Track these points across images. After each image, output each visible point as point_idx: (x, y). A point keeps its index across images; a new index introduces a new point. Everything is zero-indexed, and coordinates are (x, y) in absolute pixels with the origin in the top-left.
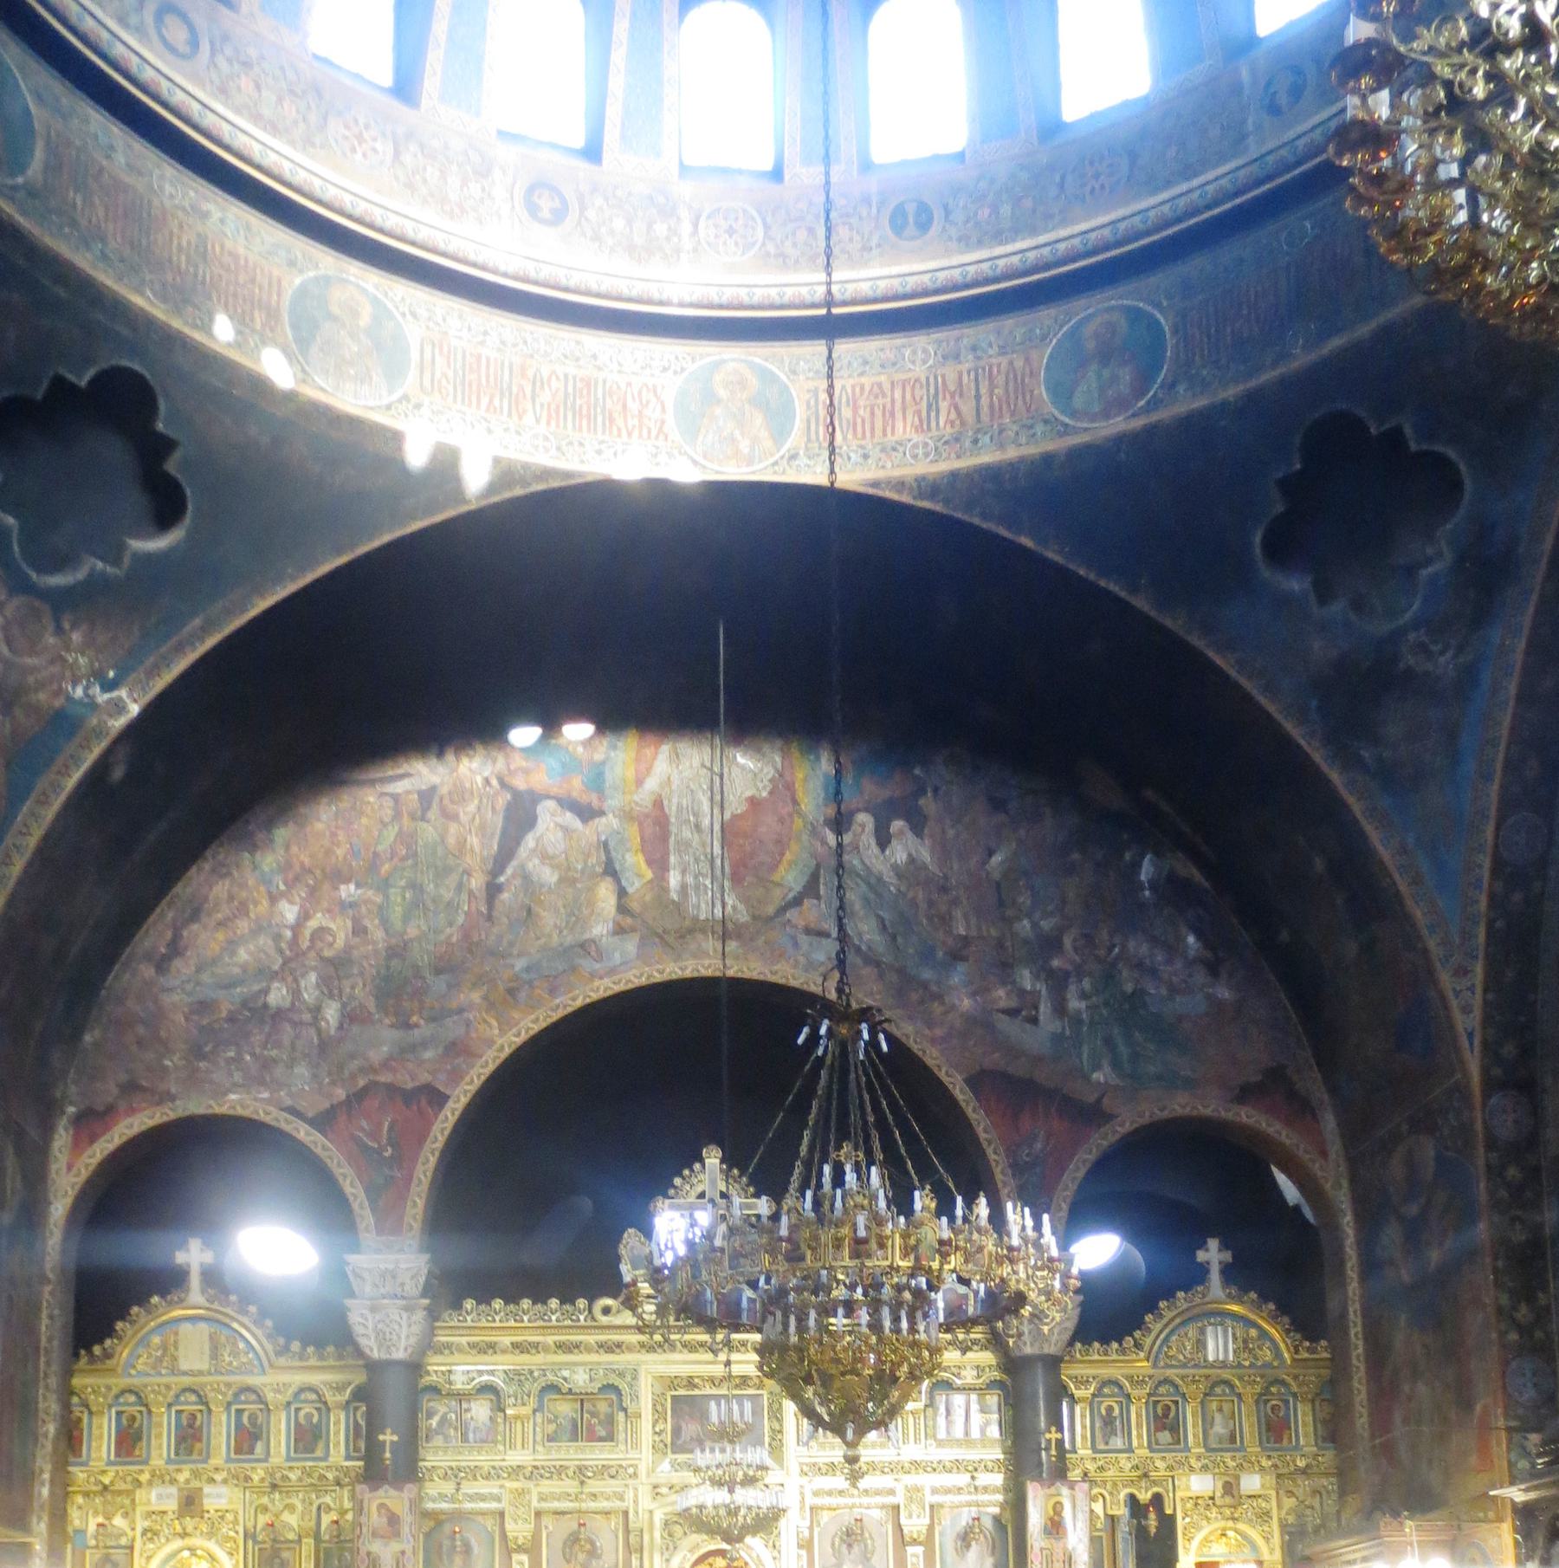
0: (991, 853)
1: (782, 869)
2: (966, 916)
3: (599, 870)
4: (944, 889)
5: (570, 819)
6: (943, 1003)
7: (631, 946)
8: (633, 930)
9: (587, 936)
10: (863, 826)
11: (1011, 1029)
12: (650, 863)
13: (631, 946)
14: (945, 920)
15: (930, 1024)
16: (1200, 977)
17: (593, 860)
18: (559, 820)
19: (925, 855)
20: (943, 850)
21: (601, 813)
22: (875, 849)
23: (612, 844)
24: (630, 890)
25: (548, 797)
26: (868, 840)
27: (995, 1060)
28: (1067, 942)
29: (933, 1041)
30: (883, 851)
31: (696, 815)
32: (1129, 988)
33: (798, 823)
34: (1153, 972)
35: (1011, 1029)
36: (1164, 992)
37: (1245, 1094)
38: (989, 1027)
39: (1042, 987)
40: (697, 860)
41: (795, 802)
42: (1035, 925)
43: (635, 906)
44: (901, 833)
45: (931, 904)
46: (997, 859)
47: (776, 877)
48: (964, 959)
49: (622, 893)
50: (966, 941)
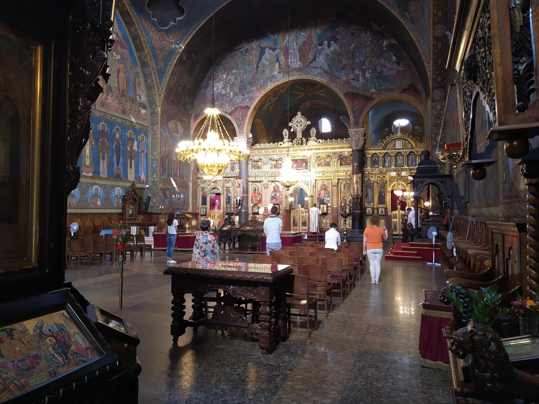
0: (351, 45)
1: (309, 55)
2: (345, 60)
3: (276, 61)
4: (341, 55)
5: (271, 51)
6: (340, 79)
7: (281, 75)
8: (282, 72)
9: (274, 74)
10: (325, 44)
11: (354, 83)
12: (285, 58)
13: (281, 75)
14: (341, 61)
15: (337, 84)
16: (395, 66)
17: (275, 59)
18: (269, 52)
19: (337, 48)
20: (341, 46)
21: (277, 49)
22: (328, 48)
23: (278, 55)
24: (281, 64)
25: (267, 48)
26: (326, 47)
27: (350, 90)
28: (366, 62)
29: (337, 87)
30: (329, 48)
31: (293, 47)
32: (379, 70)
33: (313, 45)
34: (385, 66)
35: (354, 83)
36: (387, 70)
37: (404, 91)
38: (349, 83)
39: (360, 73)
40: (293, 56)
41: (312, 41)
42: (359, 59)
43: (282, 67)
44: (333, 44)
45: (338, 58)
46: (352, 46)
47: (308, 57)
48: (344, 69)
49: (280, 65)
50: (345, 65)
